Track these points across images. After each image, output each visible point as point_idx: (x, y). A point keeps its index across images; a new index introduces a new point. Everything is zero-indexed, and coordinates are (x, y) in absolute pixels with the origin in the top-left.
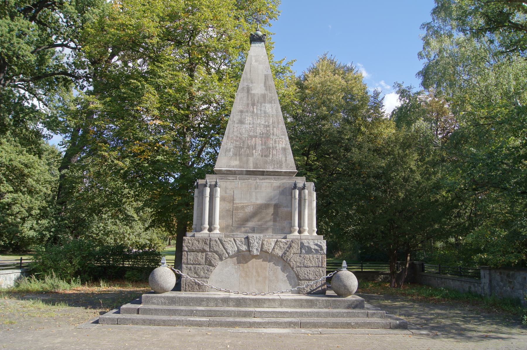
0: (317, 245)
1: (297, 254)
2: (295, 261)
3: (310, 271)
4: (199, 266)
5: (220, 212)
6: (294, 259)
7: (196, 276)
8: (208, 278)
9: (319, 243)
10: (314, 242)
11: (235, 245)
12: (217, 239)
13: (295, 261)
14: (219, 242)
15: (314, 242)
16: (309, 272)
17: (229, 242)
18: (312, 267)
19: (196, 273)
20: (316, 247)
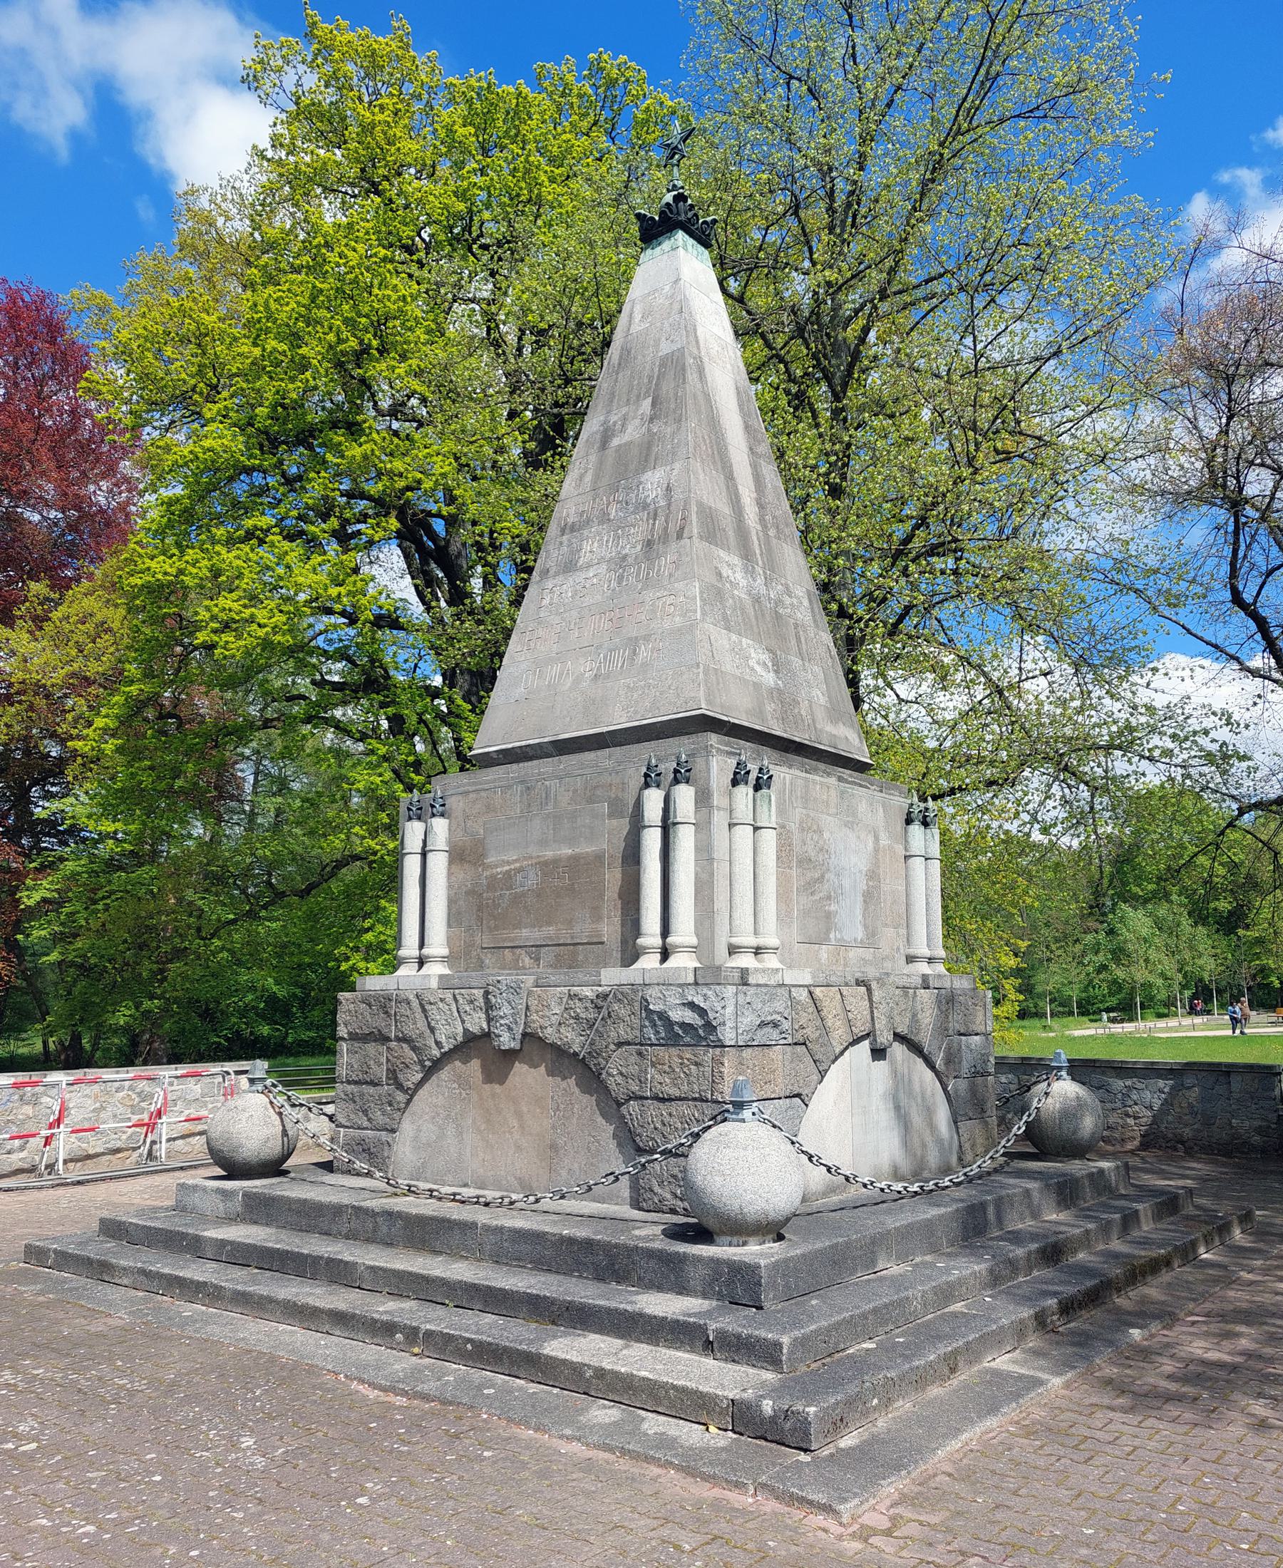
0: (692, 1006)
1: (629, 1043)
2: (621, 1074)
3: (670, 1115)
4: (371, 1090)
5: (451, 902)
6: (617, 1068)
7: (366, 1124)
8: (393, 1131)
9: (698, 1000)
10: (683, 995)
11: (456, 1014)
12: (411, 997)
13: (621, 1074)
14: (415, 1003)
15: (683, 995)
16: (667, 1119)
17: (441, 1005)
18: (680, 1099)
19: (365, 1112)
20: (689, 1017)
